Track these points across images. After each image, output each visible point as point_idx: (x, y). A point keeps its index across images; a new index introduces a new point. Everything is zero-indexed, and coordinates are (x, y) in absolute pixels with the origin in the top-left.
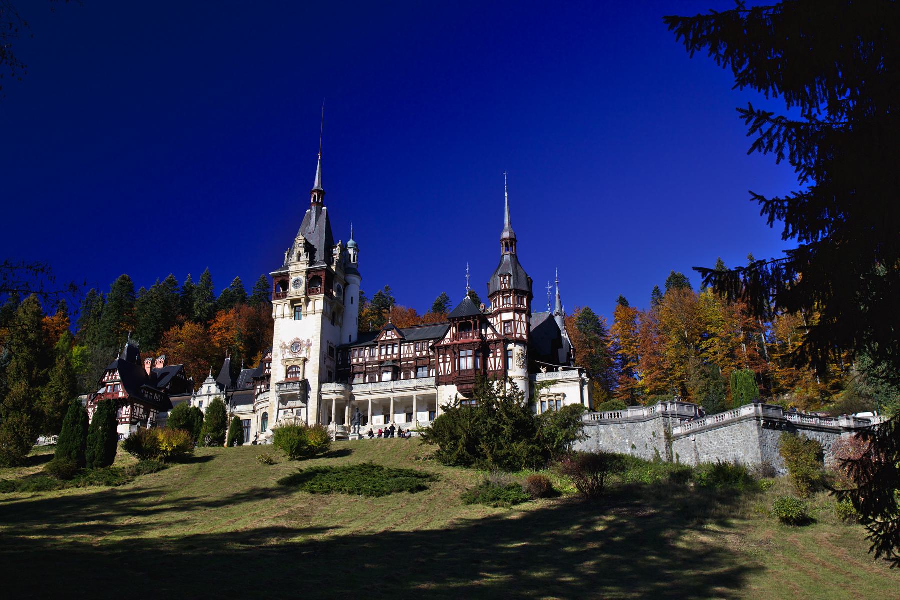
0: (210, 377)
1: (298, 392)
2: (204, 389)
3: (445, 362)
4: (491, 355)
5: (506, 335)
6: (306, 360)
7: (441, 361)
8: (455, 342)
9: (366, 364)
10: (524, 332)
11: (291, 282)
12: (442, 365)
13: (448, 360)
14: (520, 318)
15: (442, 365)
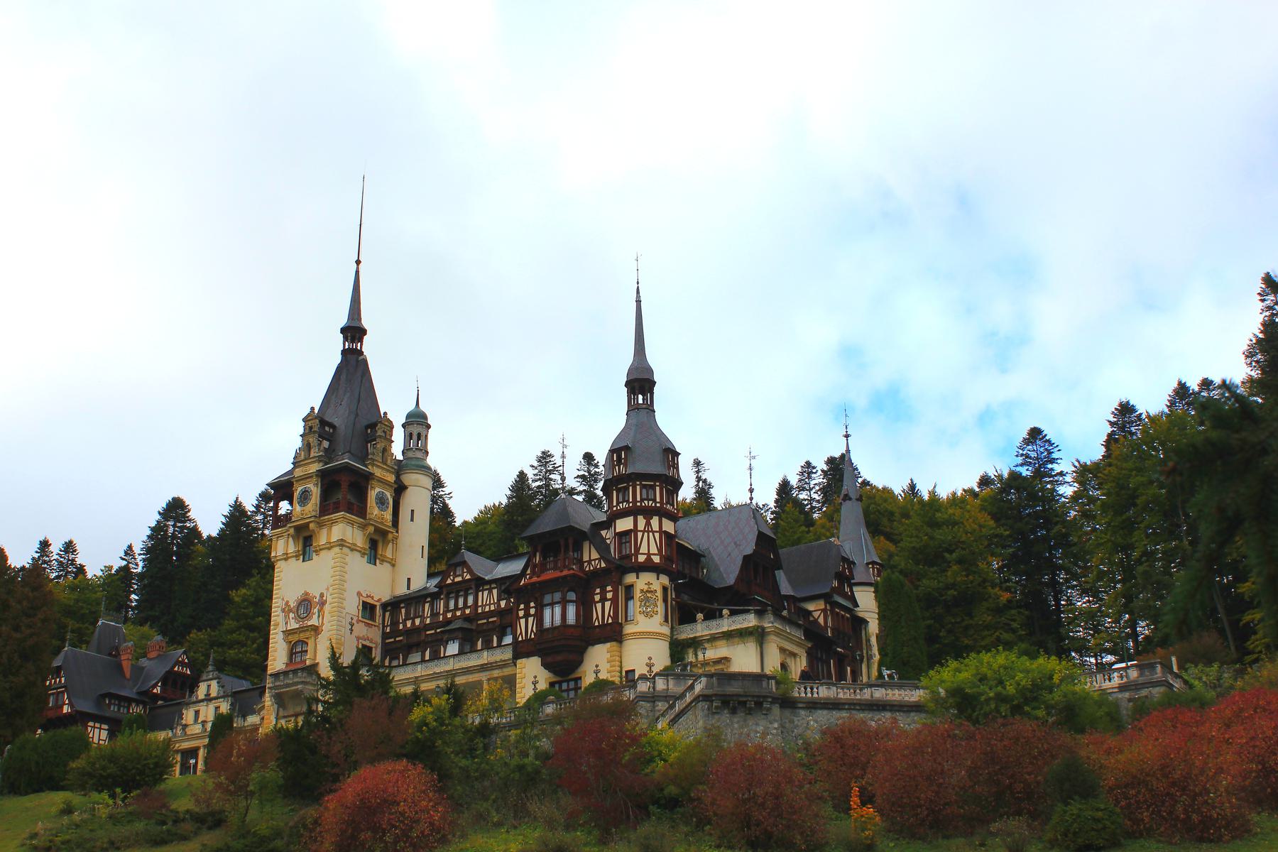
0: (210, 668)
1: (300, 687)
2: (202, 691)
3: (527, 616)
4: (597, 598)
5: (621, 558)
6: (316, 630)
7: (521, 613)
8: (535, 579)
9: (427, 627)
10: (654, 550)
11: (296, 495)
12: (523, 621)
13: (532, 611)
14: (648, 524)
15: (523, 621)
